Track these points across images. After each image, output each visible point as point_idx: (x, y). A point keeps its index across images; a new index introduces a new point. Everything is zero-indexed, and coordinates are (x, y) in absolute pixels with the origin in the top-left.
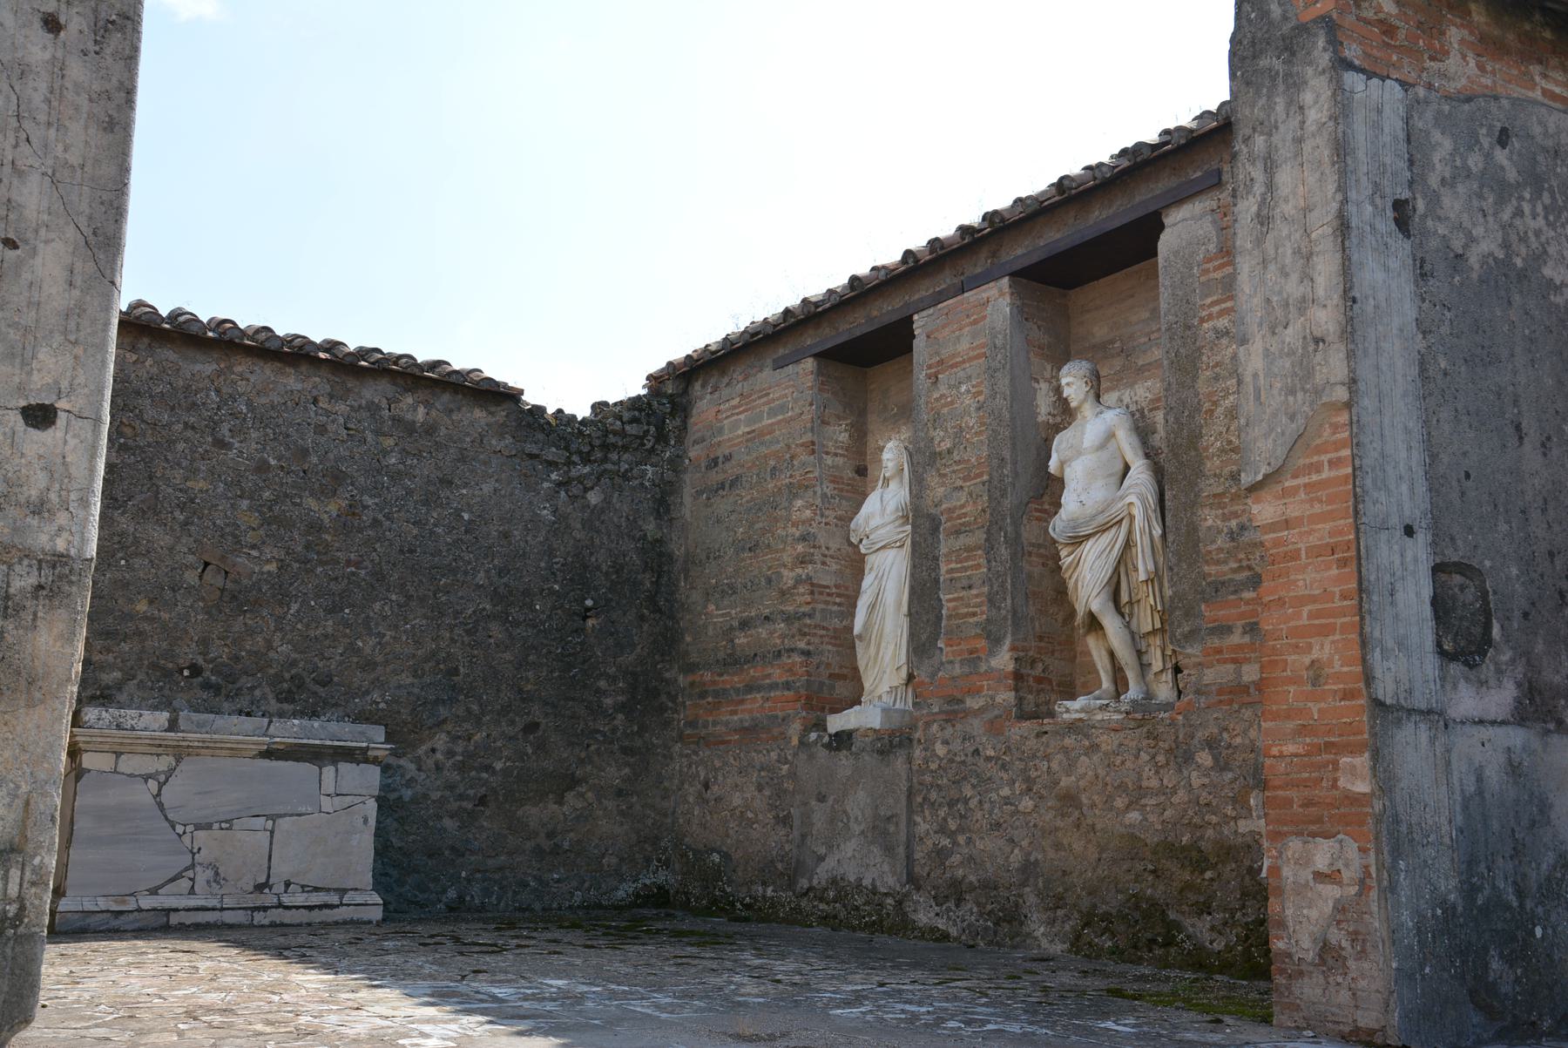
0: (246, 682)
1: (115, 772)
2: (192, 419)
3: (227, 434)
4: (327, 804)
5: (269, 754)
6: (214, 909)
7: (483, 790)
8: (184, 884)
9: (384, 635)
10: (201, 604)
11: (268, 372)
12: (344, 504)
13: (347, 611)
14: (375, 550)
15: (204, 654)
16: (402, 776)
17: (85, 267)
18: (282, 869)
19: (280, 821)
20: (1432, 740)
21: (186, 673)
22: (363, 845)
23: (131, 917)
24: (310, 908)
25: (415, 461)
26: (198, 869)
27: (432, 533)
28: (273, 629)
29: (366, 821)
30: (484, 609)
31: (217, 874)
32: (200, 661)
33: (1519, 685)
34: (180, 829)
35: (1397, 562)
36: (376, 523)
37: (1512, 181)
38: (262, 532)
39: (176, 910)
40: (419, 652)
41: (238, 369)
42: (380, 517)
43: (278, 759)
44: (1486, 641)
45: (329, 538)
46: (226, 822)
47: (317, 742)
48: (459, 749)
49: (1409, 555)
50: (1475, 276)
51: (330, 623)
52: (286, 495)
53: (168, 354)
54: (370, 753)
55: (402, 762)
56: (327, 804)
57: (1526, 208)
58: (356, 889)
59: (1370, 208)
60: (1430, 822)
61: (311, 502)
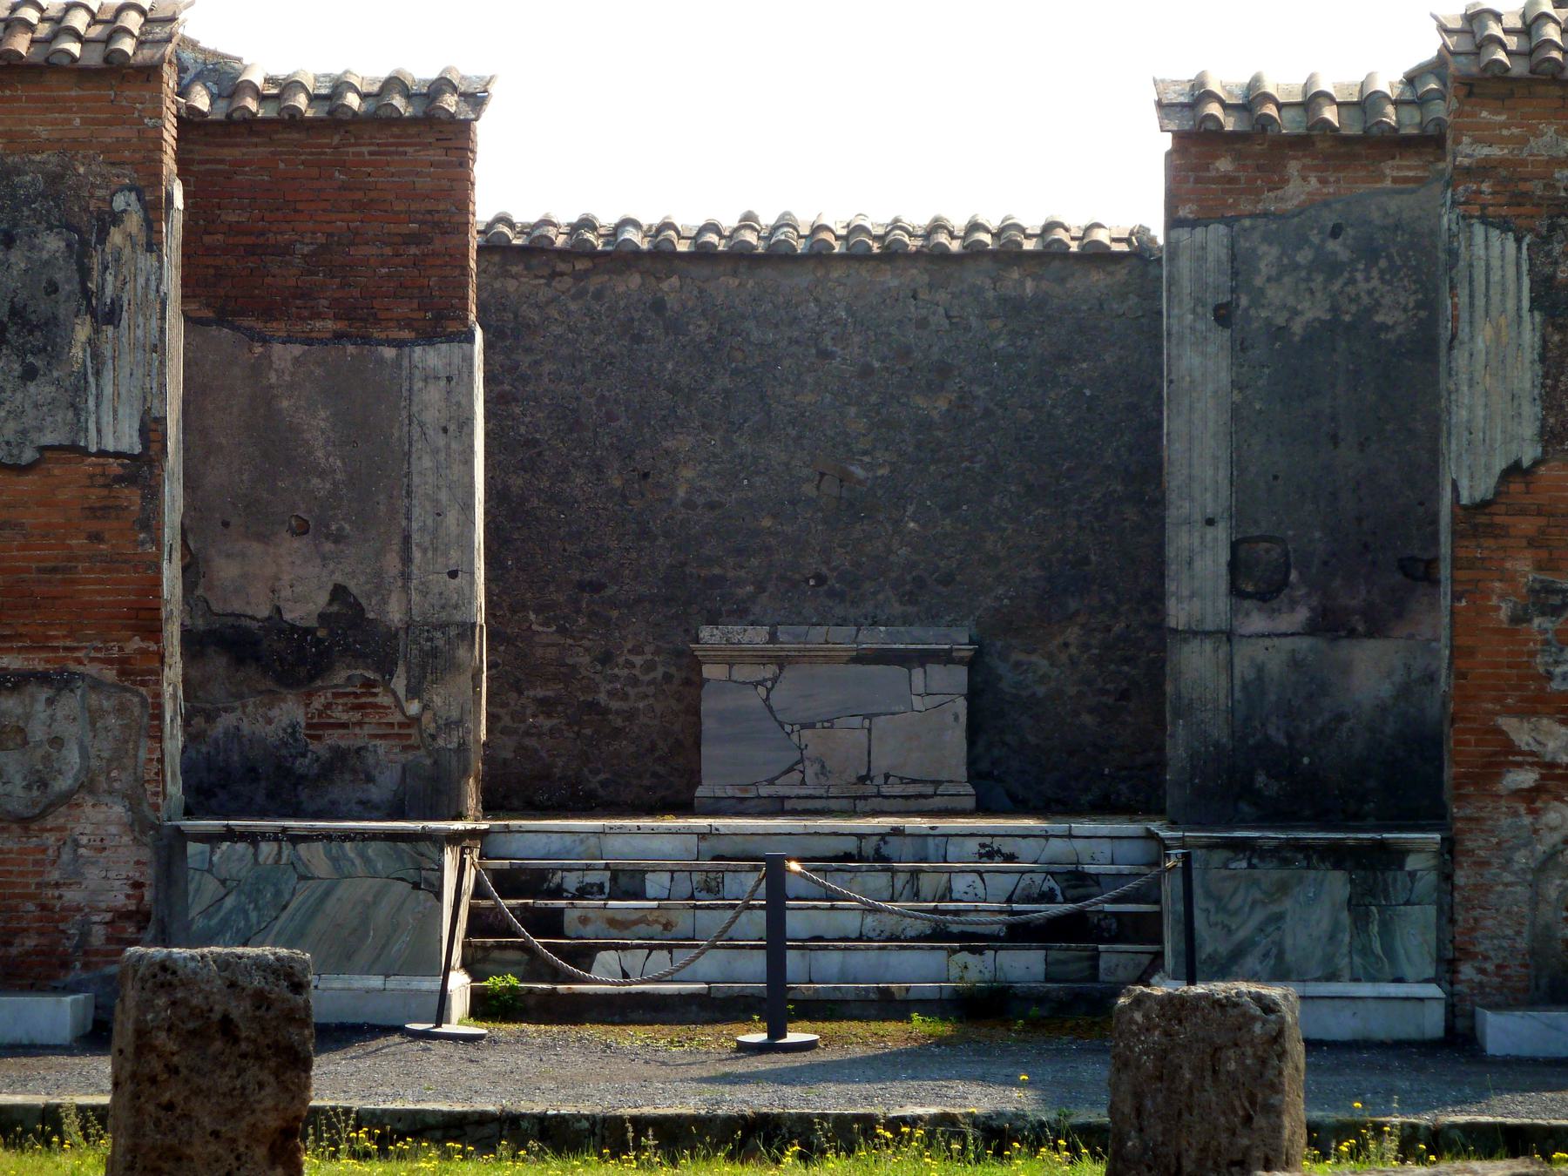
0: (868, 586)
1: (730, 680)
2: (796, 334)
3: (830, 343)
4: (917, 703)
5: (861, 658)
6: (820, 798)
7: (1124, 684)
8: (796, 776)
9: (1005, 529)
10: (820, 515)
11: (864, 273)
12: (953, 397)
13: (965, 507)
14: (989, 442)
15: (827, 563)
16: (1035, 672)
17: (462, 518)
18: (881, 764)
19: (875, 720)
20: (1216, 650)
21: (812, 582)
22: (956, 739)
23: (754, 803)
24: (907, 797)
25: (1026, 341)
26: (807, 763)
27: (1050, 415)
28: (890, 532)
29: (956, 718)
30: (1115, 491)
31: (823, 767)
32: (824, 570)
33: (1312, 609)
34: (788, 728)
35: (1197, 542)
36: (987, 413)
37: (1345, 260)
38: (872, 436)
39: (789, 798)
40: (1045, 543)
41: (835, 275)
42: (991, 405)
43: (869, 663)
44: (1285, 582)
45: (940, 434)
46: (827, 721)
47: (902, 646)
48: (1094, 642)
49: (1209, 537)
50: (1297, 338)
51: (948, 521)
52: (892, 397)
53: (768, 273)
54: (954, 654)
55: (1034, 658)
56: (917, 703)
57: (1359, 276)
58: (952, 781)
59: (1190, 317)
60: (1209, 697)
61: (920, 401)
